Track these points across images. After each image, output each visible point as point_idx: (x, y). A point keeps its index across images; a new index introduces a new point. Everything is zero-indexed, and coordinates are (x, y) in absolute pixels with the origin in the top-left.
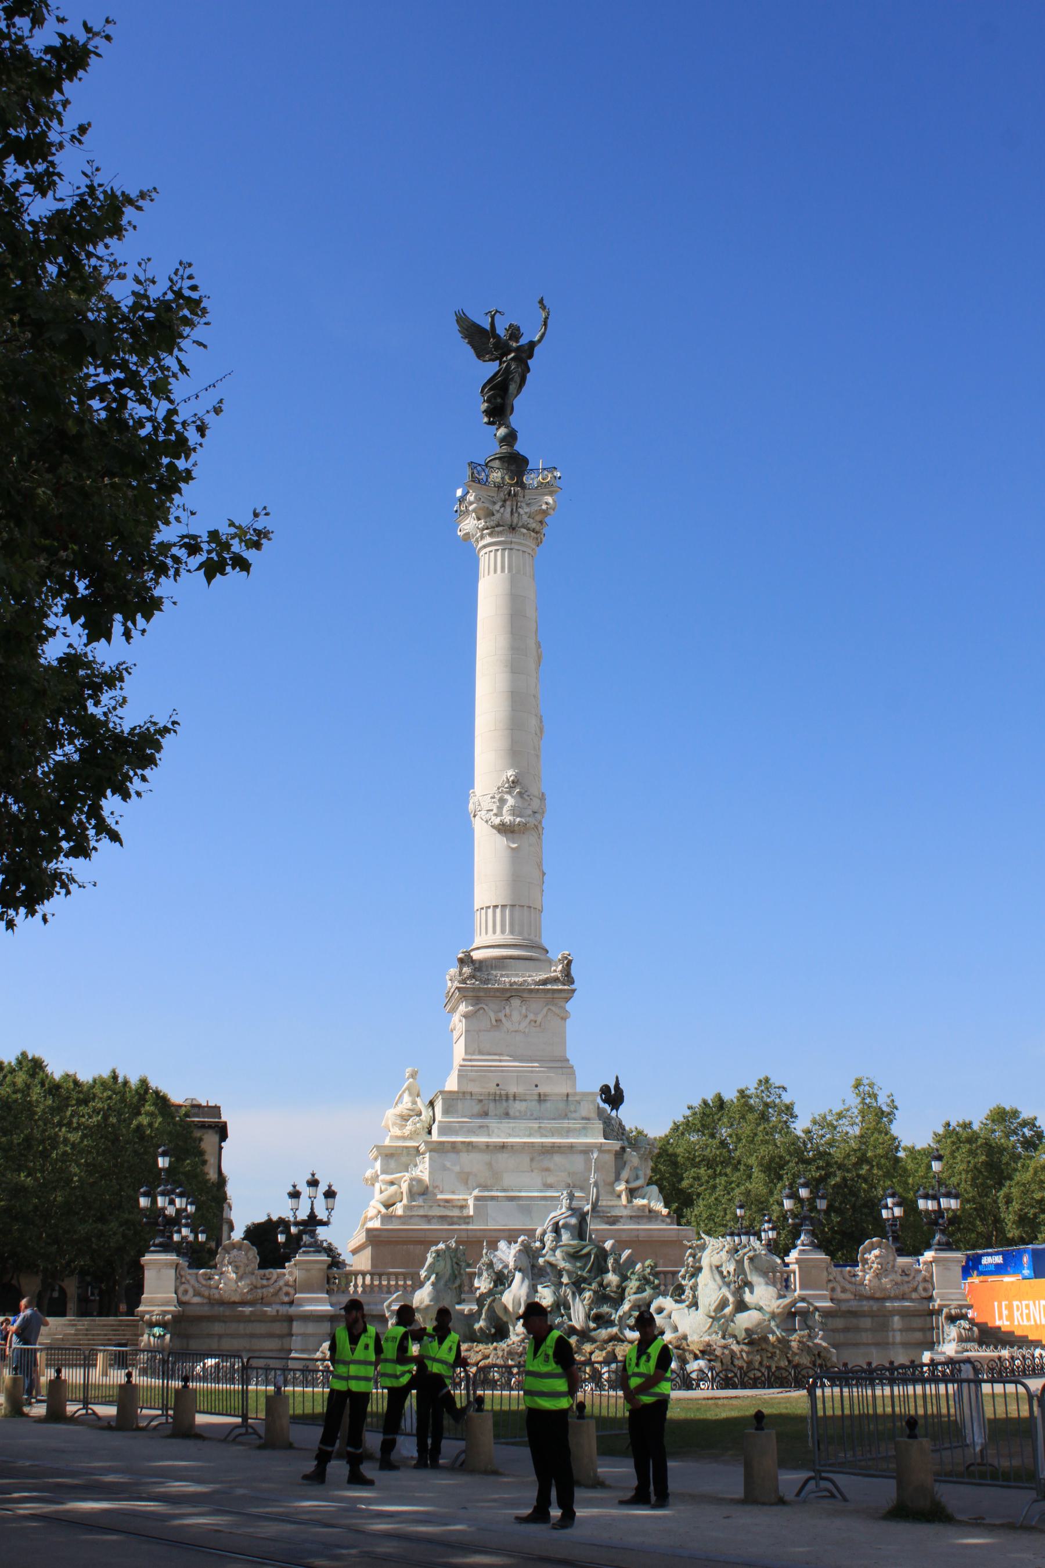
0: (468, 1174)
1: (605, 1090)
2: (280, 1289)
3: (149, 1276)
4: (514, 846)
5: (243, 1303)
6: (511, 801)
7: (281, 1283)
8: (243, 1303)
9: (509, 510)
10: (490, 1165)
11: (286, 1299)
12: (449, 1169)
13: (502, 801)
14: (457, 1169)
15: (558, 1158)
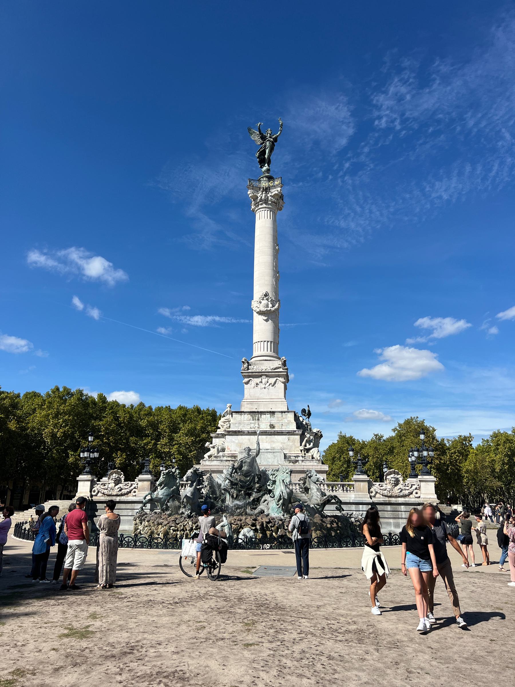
0: (241, 444)
1: (304, 411)
2: (132, 490)
3: (80, 484)
4: (266, 318)
5: (117, 495)
6: (264, 302)
7: (132, 487)
8: (117, 495)
9: (264, 195)
10: (249, 440)
11: (134, 494)
12: (234, 442)
13: (260, 302)
14: (237, 441)
15: (276, 437)
